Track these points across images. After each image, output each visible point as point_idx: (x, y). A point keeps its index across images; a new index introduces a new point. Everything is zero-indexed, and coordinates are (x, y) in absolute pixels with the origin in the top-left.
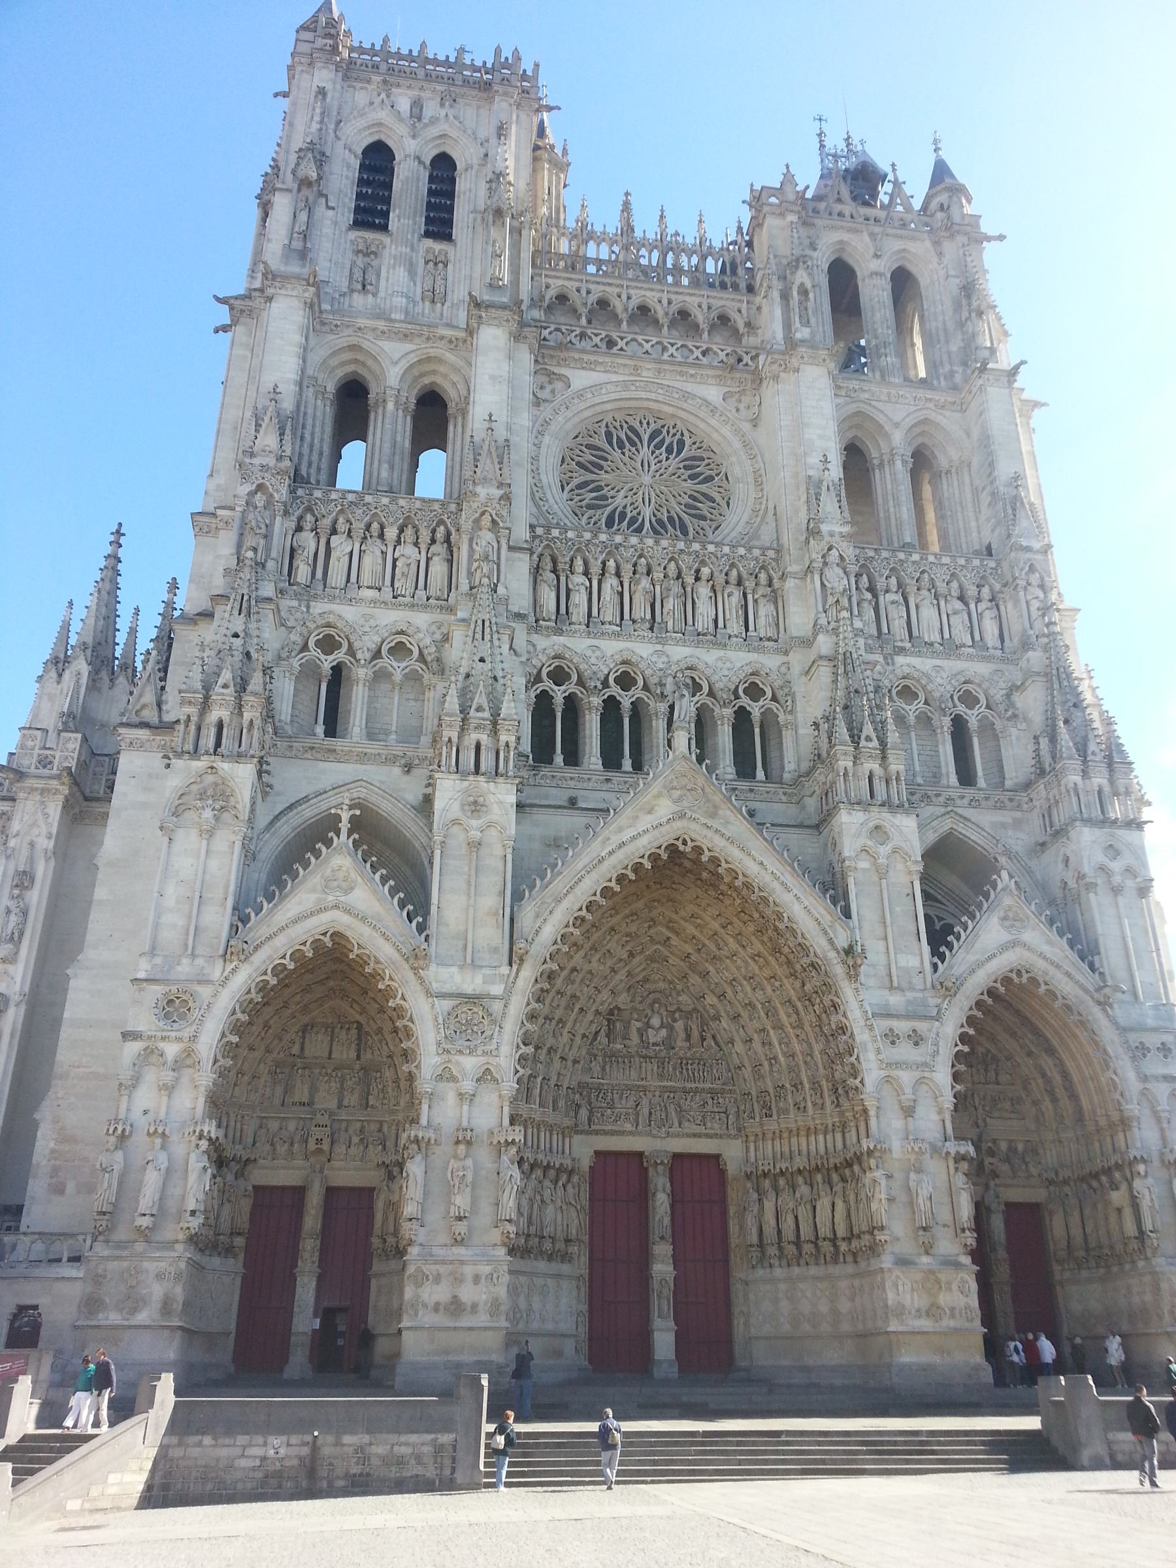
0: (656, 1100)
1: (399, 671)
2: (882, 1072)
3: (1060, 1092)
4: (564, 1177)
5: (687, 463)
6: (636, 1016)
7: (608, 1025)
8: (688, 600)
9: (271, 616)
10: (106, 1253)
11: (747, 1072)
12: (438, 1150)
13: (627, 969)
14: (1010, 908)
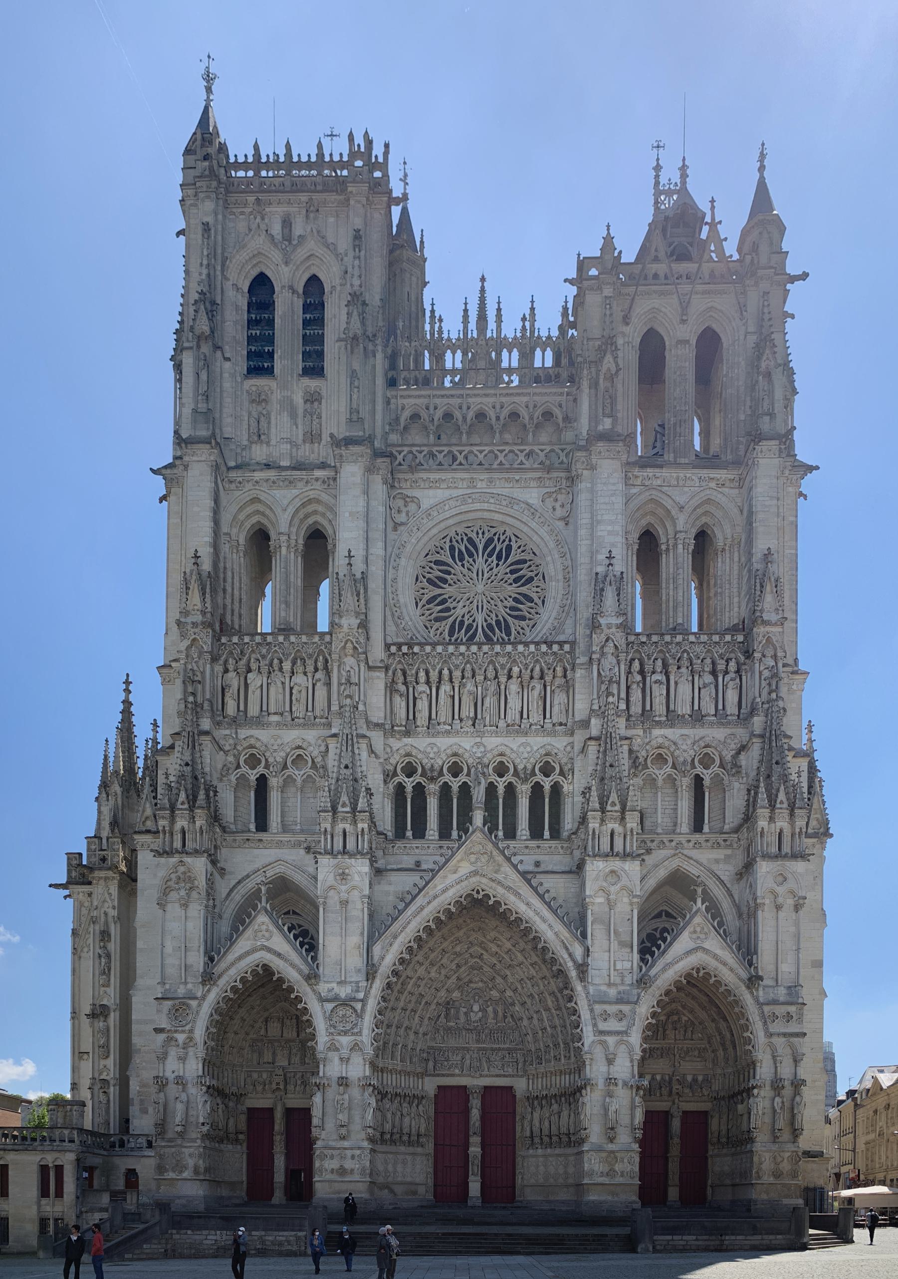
3: (728, 1043)
4: (416, 1101)
5: (512, 567)
8: (502, 696)
9: (210, 745)
10: (163, 1144)
14: (699, 924)
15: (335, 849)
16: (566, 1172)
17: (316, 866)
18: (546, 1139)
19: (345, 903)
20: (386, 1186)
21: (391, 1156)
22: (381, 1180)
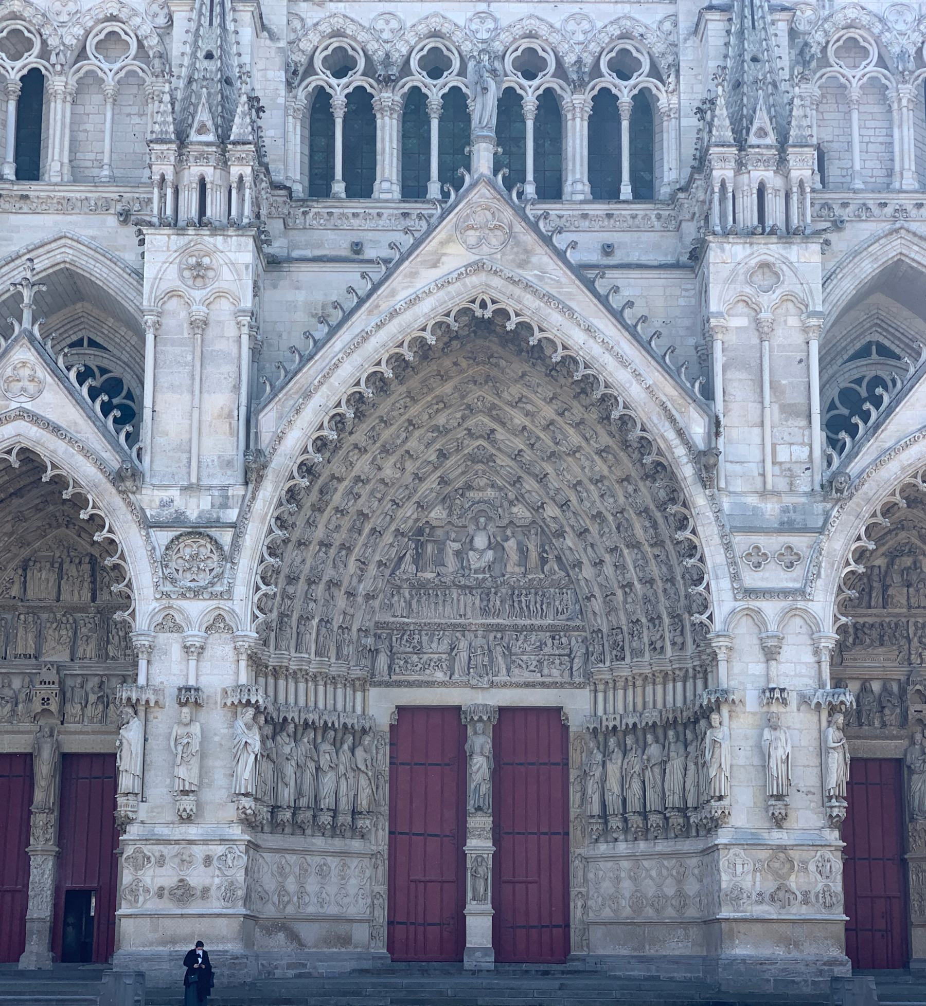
0: (480, 641)
1: (111, 75)
2: (738, 604)
4: (350, 740)
6: (453, 535)
7: (416, 548)
11: (597, 605)
12: (156, 713)
13: (438, 473)
15: (182, 216)
16: (680, 893)
17: (141, 249)
18: (636, 821)
19: (200, 325)
20: (283, 926)
21: (292, 858)
22: (269, 911)
